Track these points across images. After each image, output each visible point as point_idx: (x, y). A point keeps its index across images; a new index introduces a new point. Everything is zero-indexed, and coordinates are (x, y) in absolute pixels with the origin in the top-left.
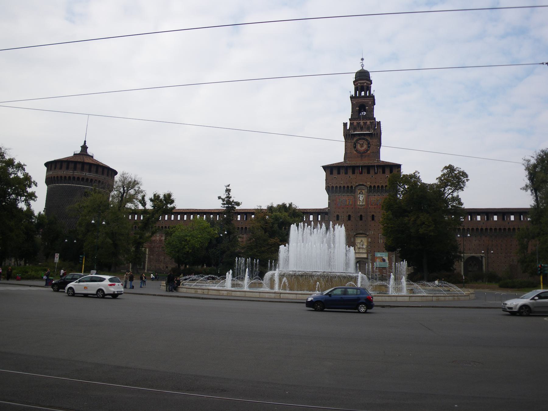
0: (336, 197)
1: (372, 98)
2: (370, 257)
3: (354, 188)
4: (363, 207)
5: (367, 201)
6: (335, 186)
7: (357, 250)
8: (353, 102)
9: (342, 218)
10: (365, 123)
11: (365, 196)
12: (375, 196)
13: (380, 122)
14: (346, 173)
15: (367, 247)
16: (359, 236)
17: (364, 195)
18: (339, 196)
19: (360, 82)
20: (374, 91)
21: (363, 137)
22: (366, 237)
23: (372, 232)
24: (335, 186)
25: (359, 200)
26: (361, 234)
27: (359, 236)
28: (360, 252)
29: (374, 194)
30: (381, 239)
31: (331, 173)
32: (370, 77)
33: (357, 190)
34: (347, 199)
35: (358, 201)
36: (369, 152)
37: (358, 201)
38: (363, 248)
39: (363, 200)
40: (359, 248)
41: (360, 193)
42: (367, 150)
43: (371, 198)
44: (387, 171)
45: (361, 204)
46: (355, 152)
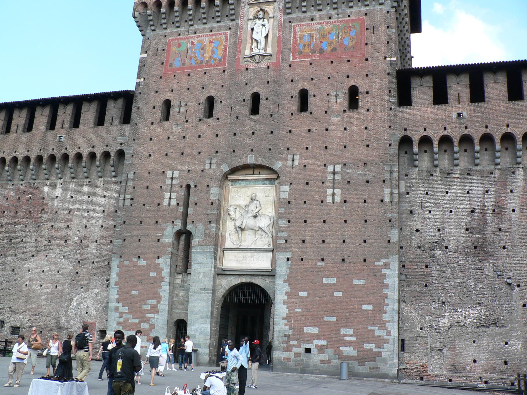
0: (168, 38)
2: (282, 269)
4: (264, 64)
5: (280, 42)
7: (234, 237)
9: (182, 109)
11: (275, 23)
12: (312, 20)
15: (275, 222)
16: (241, 177)
17: (271, 20)
18: (180, 35)
23: (297, 157)
27: (241, 177)
28: (245, 245)
29: (308, 14)
30: (334, 188)
33: (247, 7)
34: (206, 40)
35: (248, 46)
37: (248, 46)
39: (266, 37)
40: (242, 230)
41: (256, 17)
43: (298, 29)
45: (256, 51)
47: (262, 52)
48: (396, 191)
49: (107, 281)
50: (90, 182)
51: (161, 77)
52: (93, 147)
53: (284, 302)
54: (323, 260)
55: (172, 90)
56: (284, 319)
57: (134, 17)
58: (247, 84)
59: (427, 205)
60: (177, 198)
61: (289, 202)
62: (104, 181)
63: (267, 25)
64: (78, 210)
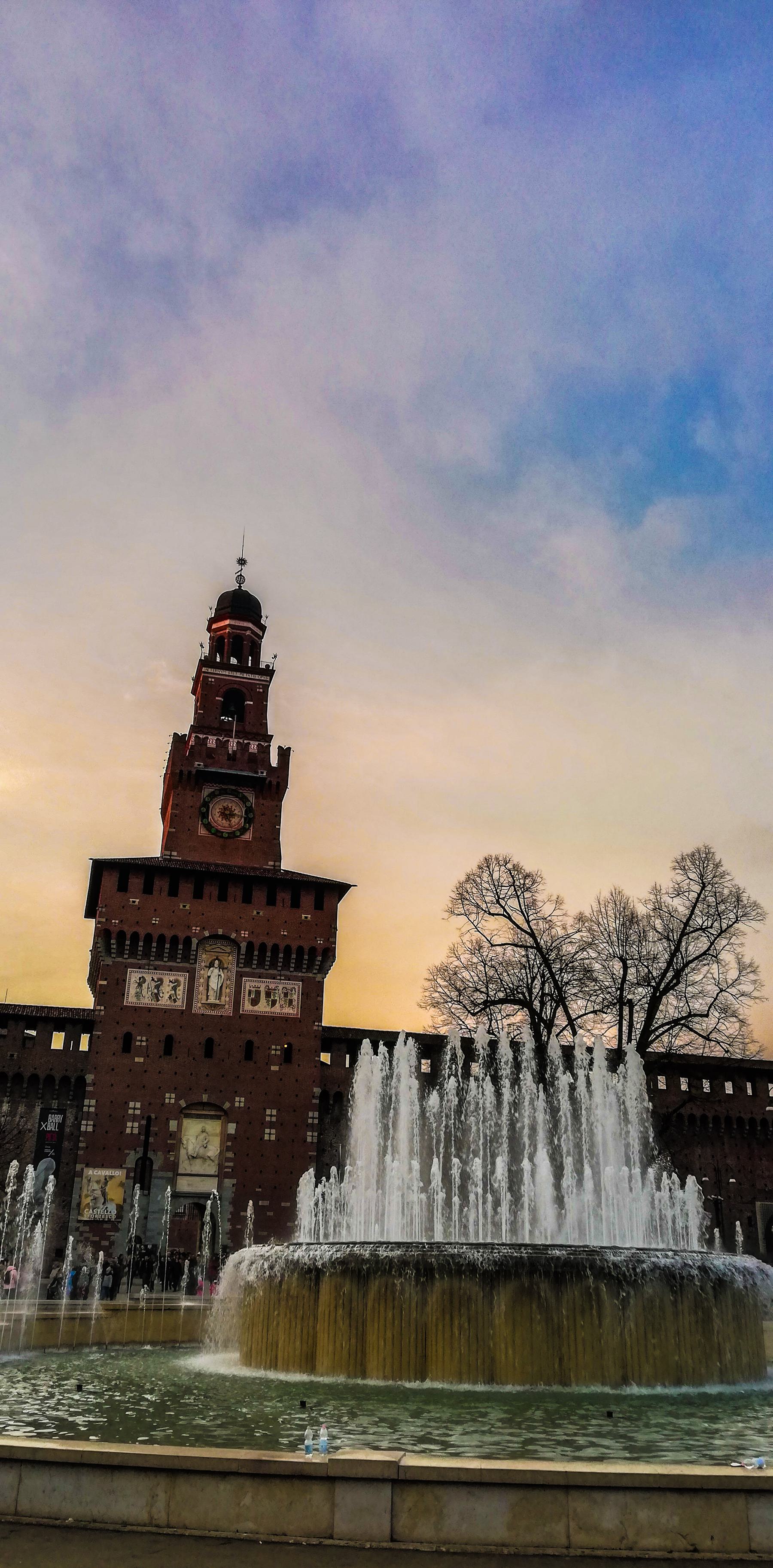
1: (269, 678)
3: (194, 947)
6: (129, 931)
10: (244, 748)
13: (289, 749)
16: (193, 1112)
17: (226, 971)
20: (275, 657)
21: (233, 788)
22: (218, 1117)
24: (129, 931)
25: (208, 986)
26: (203, 1105)
27: (193, 1112)
29: (257, 971)
31: (123, 887)
32: (262, 617)
36: (248, 836)
38: (204, 1159)
39: (221, 987)
40: (193, 1157)
42: (243, 830)
44: (307, 900)
45: (212, 1000)
46: (202, 831)
47: (217, 1002)
48: (316, 1134)
49: (63, 1202)
50: (42, 1103)
51: (122, 1009)
52: (51, 1069)
53: (229, 1220)
54: (260, 1187)
55: (133, 1024)
56: (227, 1234)
58: (202, 1029)
59: (334, 1145)
60: (140, 1127)
61: (235, 1138)
62: (58, 1103)
63: (223, 975)
64: (30, 1131)
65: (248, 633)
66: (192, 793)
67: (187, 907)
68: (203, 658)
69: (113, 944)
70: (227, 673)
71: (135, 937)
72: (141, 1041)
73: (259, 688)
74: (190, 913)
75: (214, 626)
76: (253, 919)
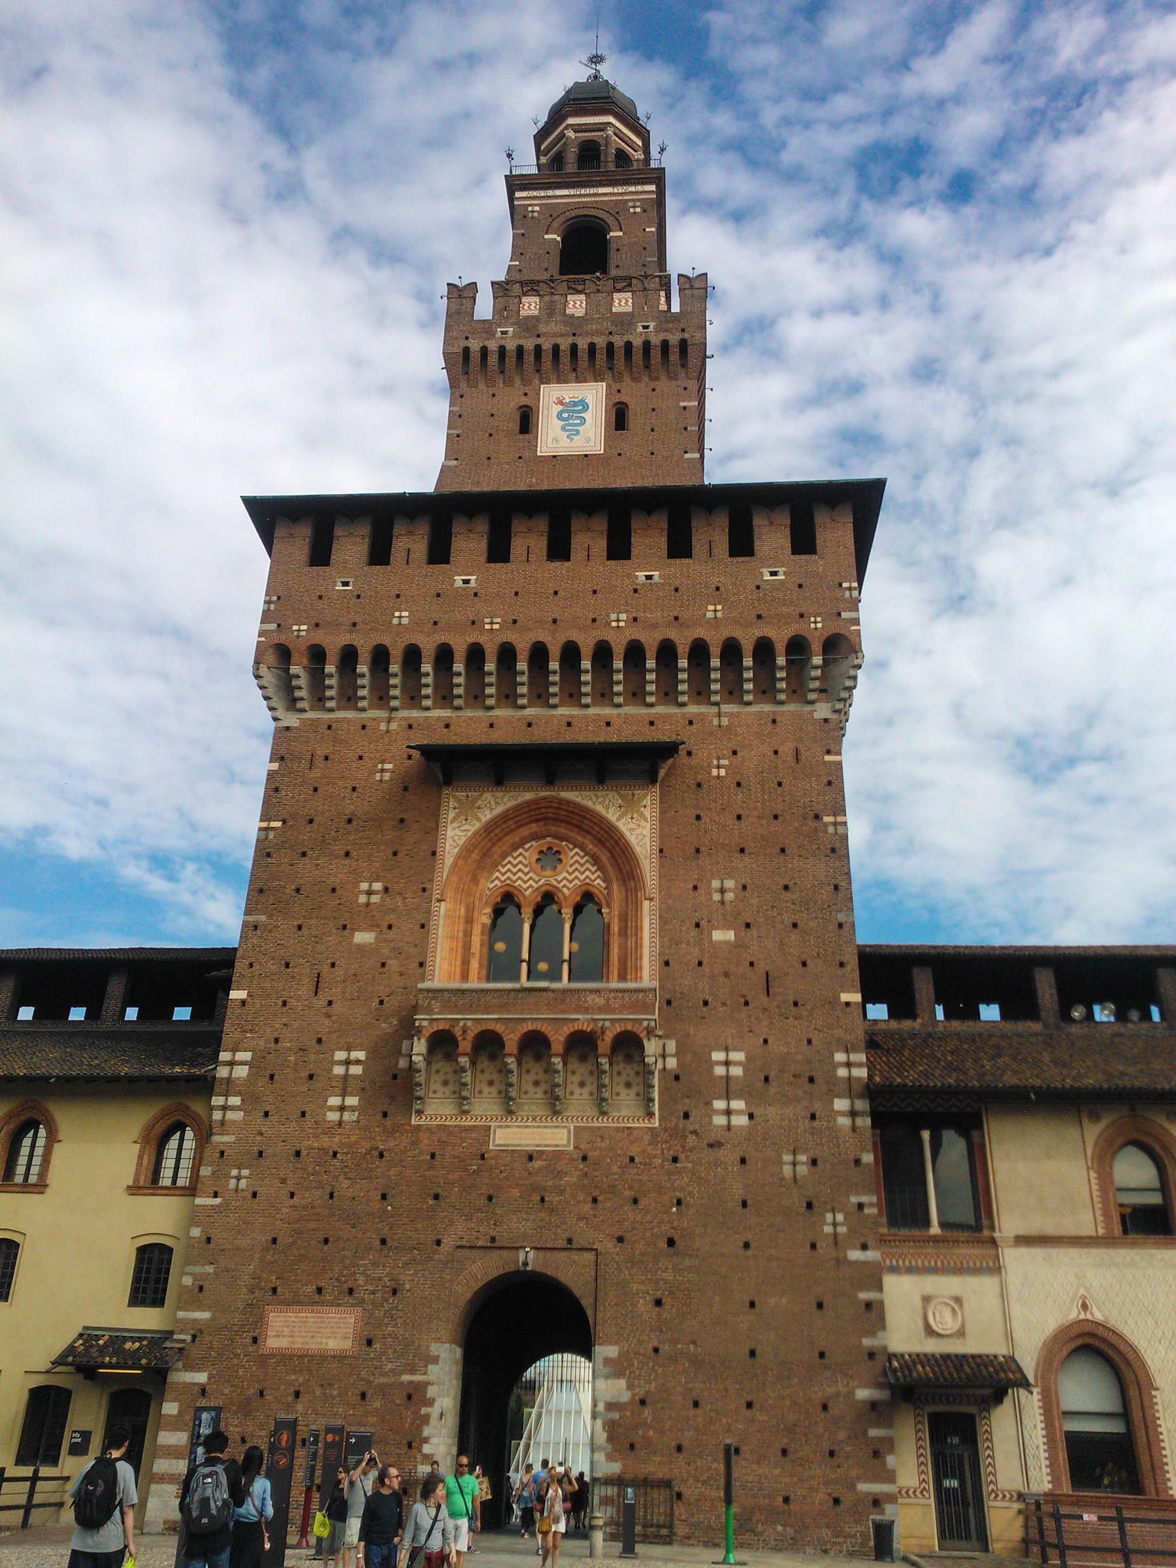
1: (653, 188)
8: (530, 205)
14: (439, 553)
19: (571, 121)
20: (662, 150)
24: (333, 644)
31: (320, 556)
32: (639, 119)
57: (257, 677)
65: (610, 132)
66: (494, 390)
67: (473, 584)
68: (515, 172)
69: (298, 677)
70: (565, 192)
71: (349, 656)
72: (369, 893)
73: (634, 207)
74: (476, 594)
75: (542, 148)
76: (636, 591)
